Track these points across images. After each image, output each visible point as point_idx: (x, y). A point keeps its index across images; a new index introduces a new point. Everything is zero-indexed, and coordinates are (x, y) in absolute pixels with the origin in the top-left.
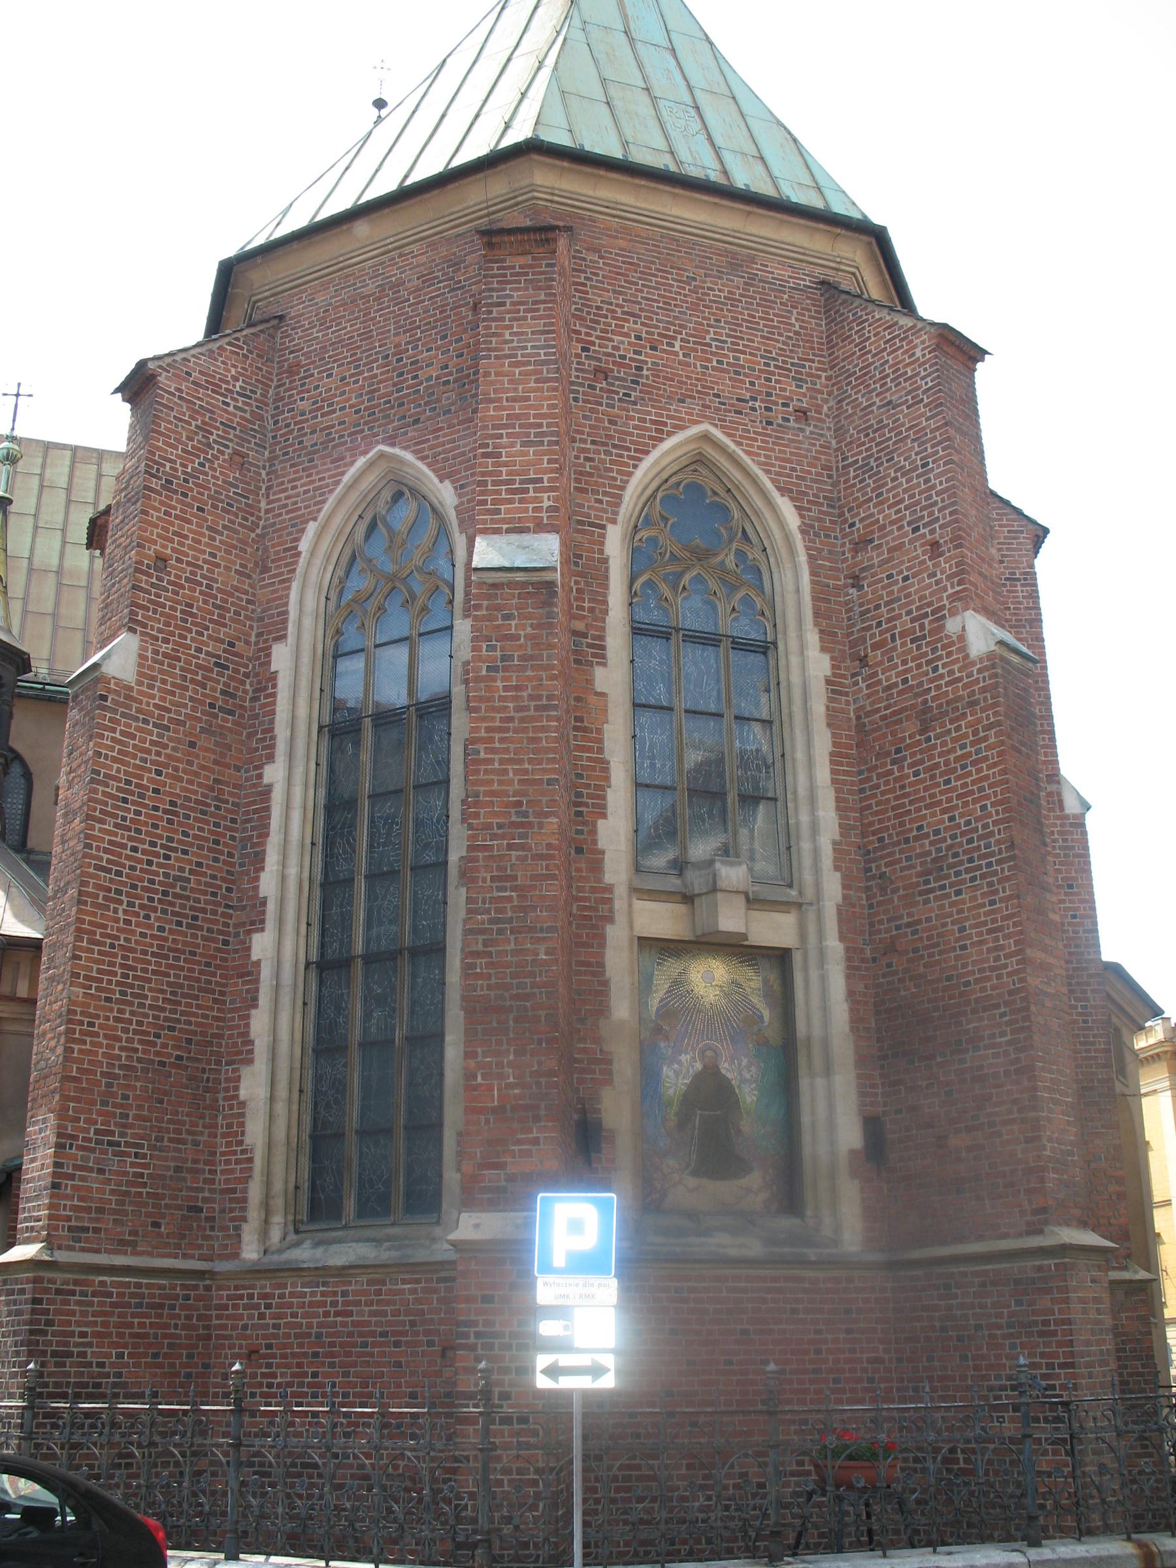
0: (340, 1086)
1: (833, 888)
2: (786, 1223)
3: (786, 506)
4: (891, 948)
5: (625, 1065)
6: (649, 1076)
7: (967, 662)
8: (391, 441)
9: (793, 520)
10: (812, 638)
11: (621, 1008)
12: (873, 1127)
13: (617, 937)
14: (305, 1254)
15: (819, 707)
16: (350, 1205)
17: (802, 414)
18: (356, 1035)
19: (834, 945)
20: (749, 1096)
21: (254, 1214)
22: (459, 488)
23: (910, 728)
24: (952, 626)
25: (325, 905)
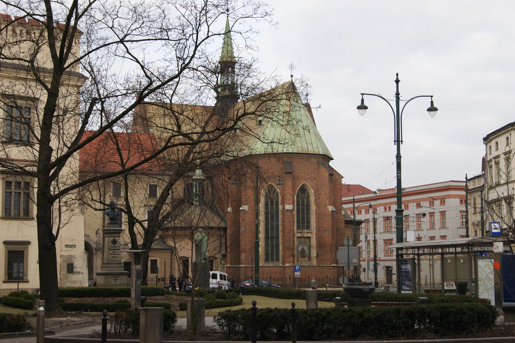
0: (269, 249)
1: (315, 231)
2: (309, 262)
3: (312, 190)
4: (320, 237)
5: (296, 249)
6: (298, 249)
7: (329, 211)
8: (272, 182)
9: (313, 192)
10: (314, 205)
11: (296, 244)
12: (317, 254)
13: (295, 237)
14: (266, 265)
15: (314, 213)
16: (270, 260)
17: (315, 179)
18: (270, 245)
19: (315, 237)
20: (306, 250)
21: (261, 261)
22: (280, 190)
23: (323, 216)
24: (328, 207)
25: (266, 231)
